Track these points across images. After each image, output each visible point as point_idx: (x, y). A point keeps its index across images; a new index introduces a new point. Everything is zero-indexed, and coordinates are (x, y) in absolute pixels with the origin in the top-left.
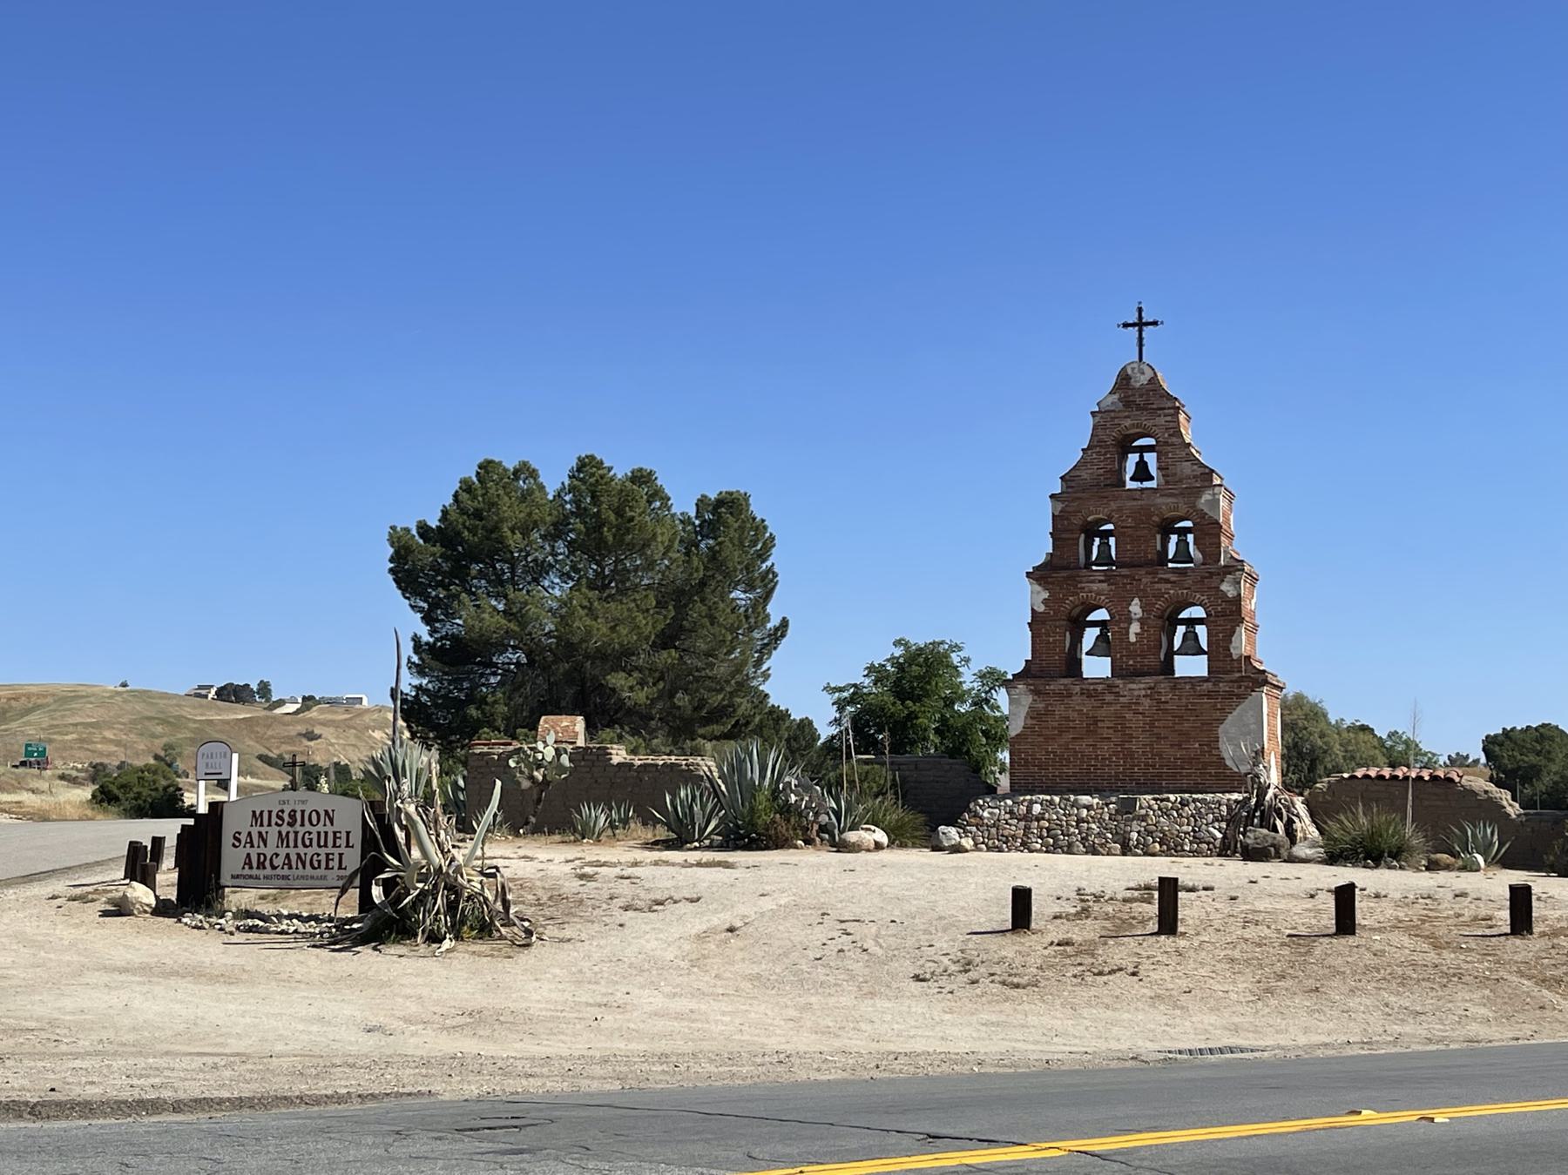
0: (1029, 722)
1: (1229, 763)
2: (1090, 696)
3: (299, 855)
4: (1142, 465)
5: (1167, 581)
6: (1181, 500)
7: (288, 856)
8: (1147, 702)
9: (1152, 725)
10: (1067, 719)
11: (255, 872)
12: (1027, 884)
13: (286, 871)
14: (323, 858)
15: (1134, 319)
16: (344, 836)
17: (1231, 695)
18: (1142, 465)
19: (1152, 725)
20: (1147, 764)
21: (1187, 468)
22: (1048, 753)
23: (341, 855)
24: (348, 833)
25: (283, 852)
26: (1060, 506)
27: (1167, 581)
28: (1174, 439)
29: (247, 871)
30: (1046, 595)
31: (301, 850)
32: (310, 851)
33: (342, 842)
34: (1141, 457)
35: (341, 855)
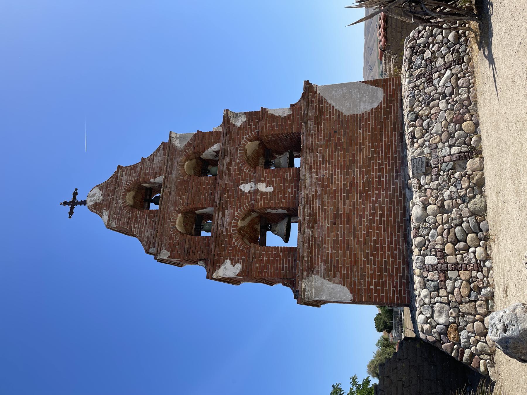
0: (338, 279)
1: (375, 105)
5: (229, 164)
8: (322, 172)
15: (68, 208)
21: (157, 160)
22: (368, 261)
27: (229, 164)
28: (138, 169)
30: (228, 262)
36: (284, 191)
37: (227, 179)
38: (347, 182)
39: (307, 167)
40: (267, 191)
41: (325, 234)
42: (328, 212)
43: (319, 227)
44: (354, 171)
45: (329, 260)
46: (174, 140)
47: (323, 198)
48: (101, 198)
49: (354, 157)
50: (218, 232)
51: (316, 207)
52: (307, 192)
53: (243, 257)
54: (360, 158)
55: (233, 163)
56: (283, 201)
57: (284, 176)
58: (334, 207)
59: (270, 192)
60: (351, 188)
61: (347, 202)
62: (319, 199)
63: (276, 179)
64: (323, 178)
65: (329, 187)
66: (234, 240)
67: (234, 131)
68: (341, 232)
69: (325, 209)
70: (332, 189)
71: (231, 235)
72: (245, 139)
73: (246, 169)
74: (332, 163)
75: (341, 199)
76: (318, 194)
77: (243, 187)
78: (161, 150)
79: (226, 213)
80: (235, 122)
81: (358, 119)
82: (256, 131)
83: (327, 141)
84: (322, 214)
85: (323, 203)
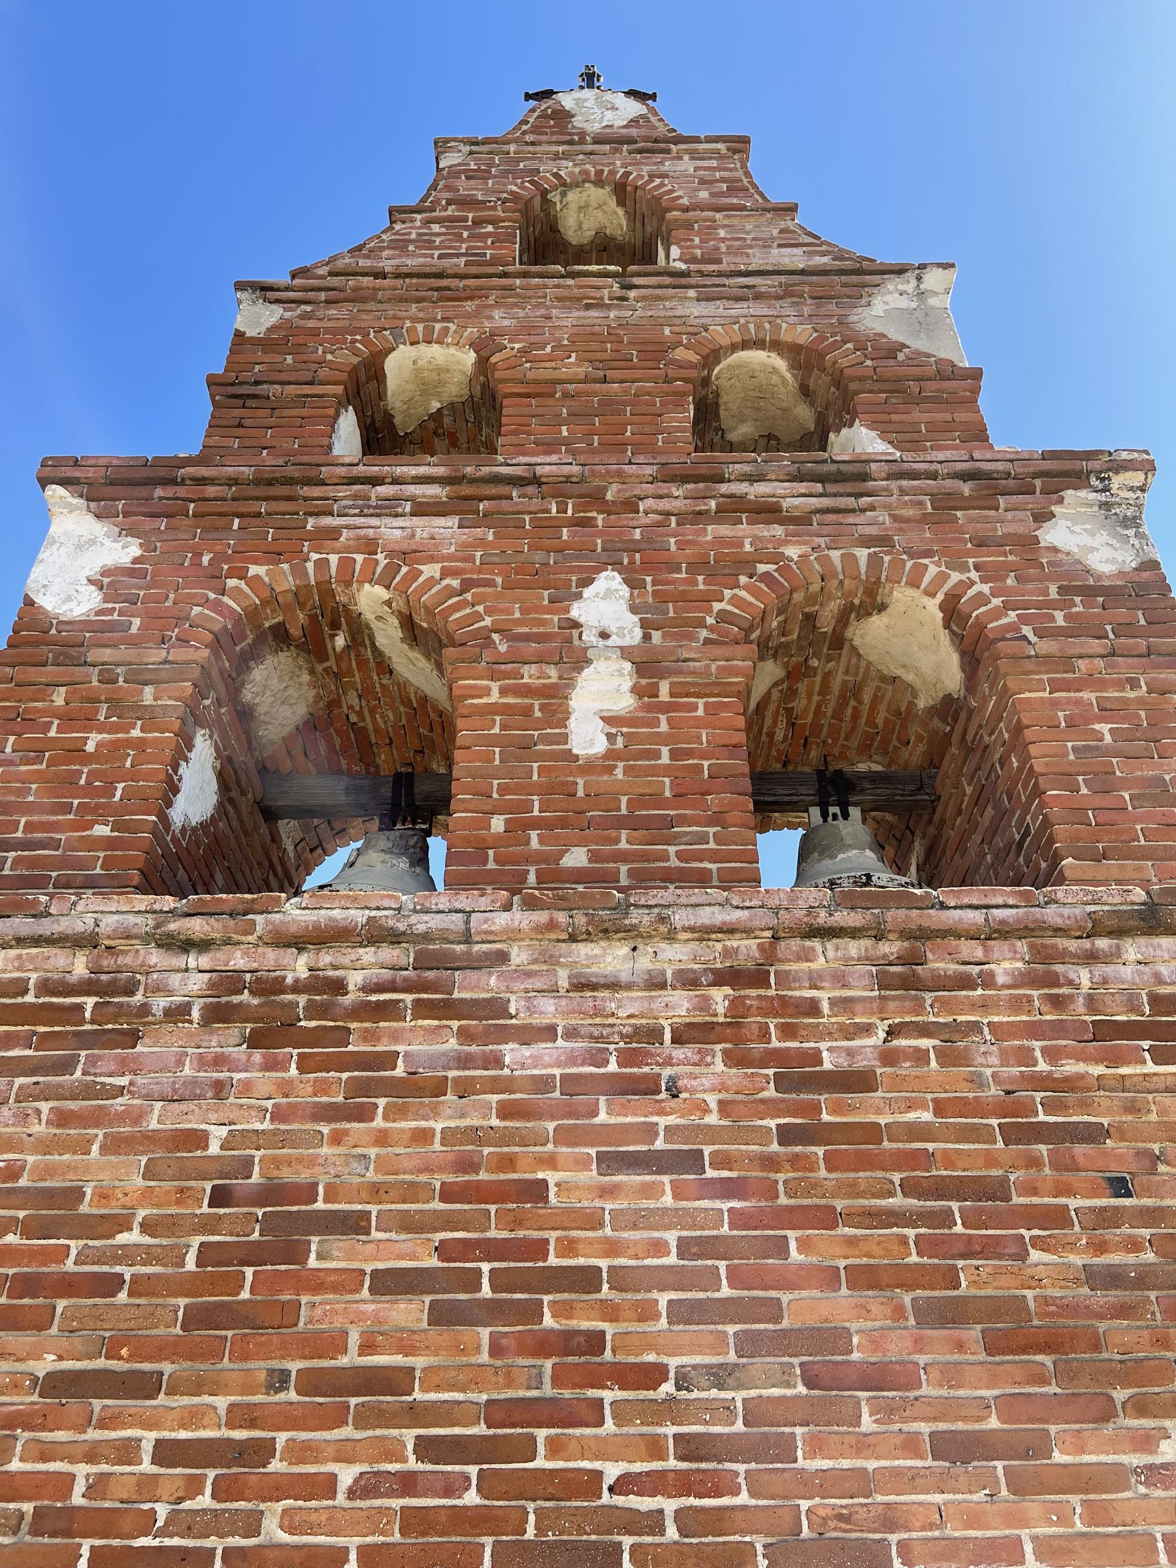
2: (272, 1033)
5: (768, 512)
27: (768, 512)
36: (571, 820)
37: (665, 505)
38: (611, 1312)
39: (748, 948)
40: (572, 723)
41: (138, 1117)
42: (337, 1139)
43: (219, 1061)
44: (720, 1376)
46: (910, 287)
47: (465, 1090)
49: (876, 1378)
50: (316, 491)
51: (395, 1037)
52: (519, 956)
53: (137, 622)
54: (864, 1445)
56: (498, 824)
57: (683, 820)
58: (377, 1192)
59: (564, 738)
60: (544, 1345)
61: (410, 1312)
62: (464, 1061)
63: (666, 770)
64: (649, 1087)
65: (565, 1136)
66: (254, 570)
67: (1009, 517)
68: (128, 1254)
69: (364, 1114)
70: (551, 1162)
72: (955, 577)
73: (735, 601)
74: (795, 1161)
75: (442, 1250)
76: (511, 1052)
77: (609, 594)
79: (440, 521)
80: (1075, 519)
82: (1027, 631)
83: (1011, 1104)
84: (322, 1088)
85: (422, 1088)
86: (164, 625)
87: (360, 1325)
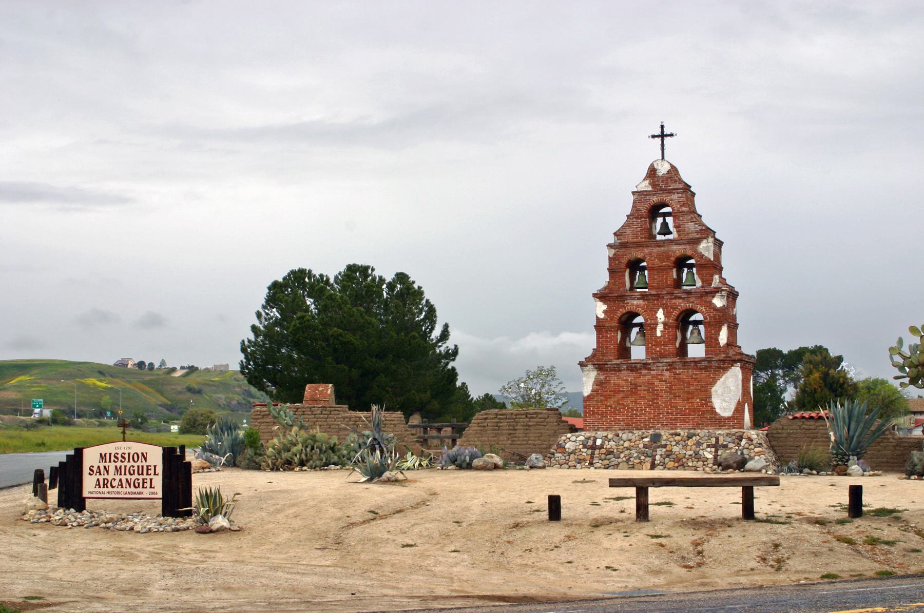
1: (718, 410)
2: (632, 371)
3: (127, 480)
4: (665, 225)
6: (688, 246)
7: (120, 480)
8: (667, 374)
9: (671, 389)
10: (619, 385)
11: (102, 490)
12: (556, 493)
13: (120, 489)
14: (141, 481)
16: (153, 468)
17: (719, 368)
18: (665, 225)
19: (671, 389)
20: (668, 413)
21: (692, 227)
22: (607, 406)
23: (151, 480)
24: (155, 467)
25: (118, 477)
26: (613, 251)
27: (680, 298)
29: (97, 489)
30: (605, 307)
31: (128, 476)
32: (133, 477)
33: (152, 472)
34: (664, 220)
35: (151, 480)
45: (607, 381)
48: (660, 174)
55: (680, 301)
71: (624, 307)
78: (700, 228)
81: (707, 398)
86: (612, 319)
87: (643, 393)
